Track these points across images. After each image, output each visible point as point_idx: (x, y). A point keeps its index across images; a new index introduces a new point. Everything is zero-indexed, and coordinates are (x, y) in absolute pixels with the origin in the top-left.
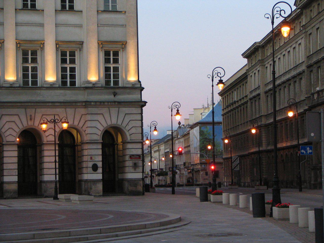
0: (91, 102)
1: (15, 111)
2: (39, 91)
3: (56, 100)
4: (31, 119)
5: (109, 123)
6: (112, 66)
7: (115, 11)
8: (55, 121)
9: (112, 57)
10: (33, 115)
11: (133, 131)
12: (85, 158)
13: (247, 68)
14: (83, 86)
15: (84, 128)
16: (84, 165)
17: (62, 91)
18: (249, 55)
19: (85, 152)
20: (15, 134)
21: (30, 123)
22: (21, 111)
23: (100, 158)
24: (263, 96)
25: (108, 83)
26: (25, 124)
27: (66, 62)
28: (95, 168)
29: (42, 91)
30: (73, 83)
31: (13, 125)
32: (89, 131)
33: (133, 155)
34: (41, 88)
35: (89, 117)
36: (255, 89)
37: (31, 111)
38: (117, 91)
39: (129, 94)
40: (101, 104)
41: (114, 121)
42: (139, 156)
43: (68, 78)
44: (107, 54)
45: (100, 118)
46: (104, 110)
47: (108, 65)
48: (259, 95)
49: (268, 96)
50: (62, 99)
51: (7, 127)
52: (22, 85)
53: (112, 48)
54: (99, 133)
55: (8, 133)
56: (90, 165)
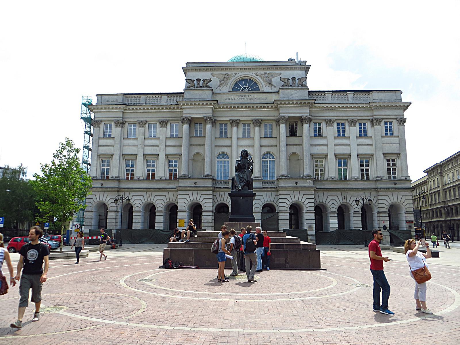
0: (381, 189)
1: (335, 194)
2: (349, 183)
3: (359, 188)
4: (345, 199)
5: (392, 201)
7: (392, 135)
8: (363, 199)
9: (391, 163)
10: (346, 196)
11: (408, 206)
13: (427, 177)
14: (375, 179)
15: (376, 204)
17: (362, 182)
18: (428, 172)
20: (335, 207)
21: (344, 201)
22: (339, 194)
24: (441, 191)
25: (389, 178)
26: (341, 201)
29: (351, 182)
30: (368, 178)
31: (334, 202)
33: (408, 221)
34: (350, 180)
35: (380, 198)
37: (344, 194)
38: (396, 182)
39: (404, 184)
40: (388, 189)
41: (395, 200)
42: (412, 221)
43: (365, 174)
44: (388, 161)
45: (386, 198)
46: (389, 194)
47: (389, 167)
48: (439, 190)
49: (446, 192)
50: (362, 187)
51: (331, 203)
52: (338, 179)
53: (391, 157)
55: (332, 206)
56: (382, 226)
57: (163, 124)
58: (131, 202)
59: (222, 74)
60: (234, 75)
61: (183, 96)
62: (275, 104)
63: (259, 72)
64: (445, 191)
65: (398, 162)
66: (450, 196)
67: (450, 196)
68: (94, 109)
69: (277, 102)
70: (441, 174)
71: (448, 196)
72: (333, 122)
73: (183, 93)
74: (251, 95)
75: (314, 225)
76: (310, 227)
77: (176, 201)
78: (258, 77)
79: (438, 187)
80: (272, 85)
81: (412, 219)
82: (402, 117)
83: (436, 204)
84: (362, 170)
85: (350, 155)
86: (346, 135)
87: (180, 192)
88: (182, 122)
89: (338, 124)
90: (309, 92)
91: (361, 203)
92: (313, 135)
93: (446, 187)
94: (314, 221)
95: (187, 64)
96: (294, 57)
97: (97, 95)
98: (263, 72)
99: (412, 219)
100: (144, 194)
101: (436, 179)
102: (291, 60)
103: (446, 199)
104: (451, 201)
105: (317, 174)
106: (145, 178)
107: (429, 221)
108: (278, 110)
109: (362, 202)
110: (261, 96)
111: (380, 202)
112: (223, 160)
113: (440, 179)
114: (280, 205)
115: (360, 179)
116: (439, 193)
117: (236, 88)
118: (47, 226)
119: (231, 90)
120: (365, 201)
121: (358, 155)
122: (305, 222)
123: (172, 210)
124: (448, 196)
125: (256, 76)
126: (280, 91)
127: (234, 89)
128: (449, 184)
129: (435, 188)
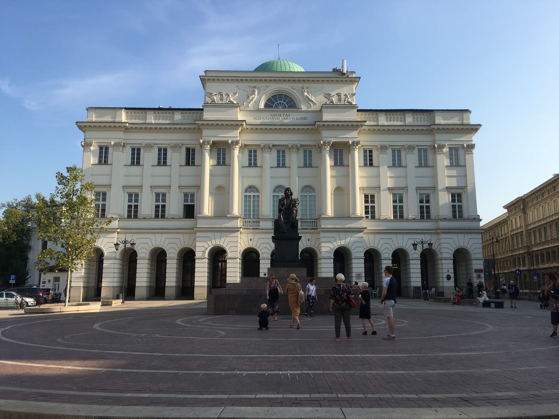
6: (457, 204)
8: (422, 242)
12: (440, 271)
16: (441, 275)
18: (509, 207)
19: (440, 266)
23: (452, 271)
27: (423, 202)
28: (449, 278)
31: (388, 246)
32: (443, 250)
34: (408, 220)
35: (443, 241)
36: (517, 229)
48: (522, 231)
49: (530, 233)
54: (450, 252)
56: (445, 275)
57: (176, 147)
58: (136, 248)
59: (251, 87)
60: (265, 88)
61: (202, 114)
62: (316, 125)
63: (295, 85)
64: (529, 232)
65: (464, 197)
66: (535, 239)
67: (535, 239)
68: (85, 126)
69: (317, 123)
70: (524, 211)
71: (533, 238)
72: (387, 148)
73: (202, 110)
74: (287, 114)
75: (363, 275)
76: (359, 276)
77: (193, 245)
78: (295, 91)
79: (521, 227)
80: (312, 101)
81: (481, 267)
82: (470, 143)
83: (519, 249)
84: (422, 207)
85: (406, 188)
86: (403, 164)
87: (198, 234)
88: (201, 147)
89: (393, 151)
90: (358, 111)
91: (419, 248)
92: (363, 164)
93: (530, 227)
94: (363, 270)
95: (206, 72)
96: (339, 67)
97: (87, 110)
98: (300, 85)
99: (481, 267)
100: (152, 236)
101: (518, 217)
102: (335, 70)
103: (531, 242)
104: (536, 245)
105: (367, 212)
106: (153, 216)
107: (510, 271)
108: (320, 133)
109: (421, 246)
110: (299, 115)
111: (443, 246)
112: (252, 194)
113: (523, 217)
114: (323, 249)
115: (419, 218)
116: (522, 235)
117: (269, 104)
118: (13, 279)
119: (262, 106)
120: (424, 245)
121: (418, 189)
122: (354, 270)
123: (187, 258)
124: (533, 238)
125: (293, 90)
126: (324, 110)
127: (266, 105)
128: (533, 223)
129: (517, 229)
